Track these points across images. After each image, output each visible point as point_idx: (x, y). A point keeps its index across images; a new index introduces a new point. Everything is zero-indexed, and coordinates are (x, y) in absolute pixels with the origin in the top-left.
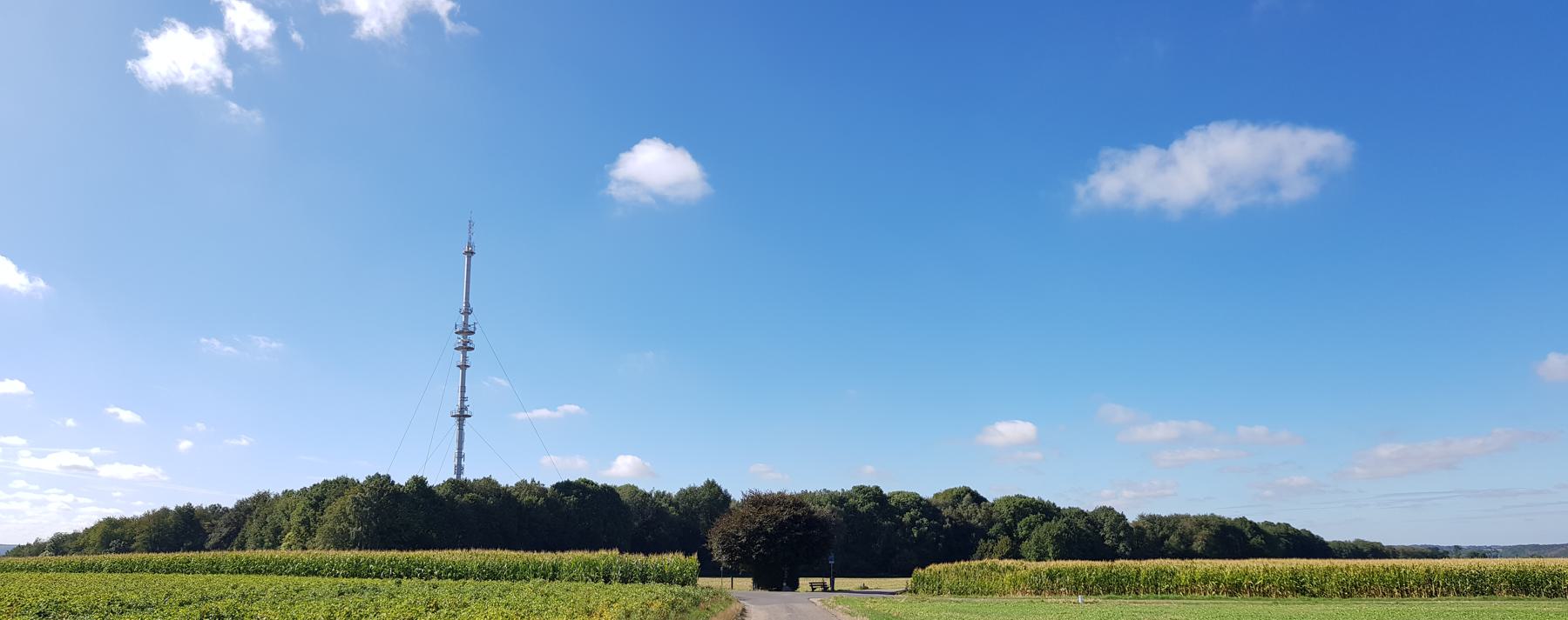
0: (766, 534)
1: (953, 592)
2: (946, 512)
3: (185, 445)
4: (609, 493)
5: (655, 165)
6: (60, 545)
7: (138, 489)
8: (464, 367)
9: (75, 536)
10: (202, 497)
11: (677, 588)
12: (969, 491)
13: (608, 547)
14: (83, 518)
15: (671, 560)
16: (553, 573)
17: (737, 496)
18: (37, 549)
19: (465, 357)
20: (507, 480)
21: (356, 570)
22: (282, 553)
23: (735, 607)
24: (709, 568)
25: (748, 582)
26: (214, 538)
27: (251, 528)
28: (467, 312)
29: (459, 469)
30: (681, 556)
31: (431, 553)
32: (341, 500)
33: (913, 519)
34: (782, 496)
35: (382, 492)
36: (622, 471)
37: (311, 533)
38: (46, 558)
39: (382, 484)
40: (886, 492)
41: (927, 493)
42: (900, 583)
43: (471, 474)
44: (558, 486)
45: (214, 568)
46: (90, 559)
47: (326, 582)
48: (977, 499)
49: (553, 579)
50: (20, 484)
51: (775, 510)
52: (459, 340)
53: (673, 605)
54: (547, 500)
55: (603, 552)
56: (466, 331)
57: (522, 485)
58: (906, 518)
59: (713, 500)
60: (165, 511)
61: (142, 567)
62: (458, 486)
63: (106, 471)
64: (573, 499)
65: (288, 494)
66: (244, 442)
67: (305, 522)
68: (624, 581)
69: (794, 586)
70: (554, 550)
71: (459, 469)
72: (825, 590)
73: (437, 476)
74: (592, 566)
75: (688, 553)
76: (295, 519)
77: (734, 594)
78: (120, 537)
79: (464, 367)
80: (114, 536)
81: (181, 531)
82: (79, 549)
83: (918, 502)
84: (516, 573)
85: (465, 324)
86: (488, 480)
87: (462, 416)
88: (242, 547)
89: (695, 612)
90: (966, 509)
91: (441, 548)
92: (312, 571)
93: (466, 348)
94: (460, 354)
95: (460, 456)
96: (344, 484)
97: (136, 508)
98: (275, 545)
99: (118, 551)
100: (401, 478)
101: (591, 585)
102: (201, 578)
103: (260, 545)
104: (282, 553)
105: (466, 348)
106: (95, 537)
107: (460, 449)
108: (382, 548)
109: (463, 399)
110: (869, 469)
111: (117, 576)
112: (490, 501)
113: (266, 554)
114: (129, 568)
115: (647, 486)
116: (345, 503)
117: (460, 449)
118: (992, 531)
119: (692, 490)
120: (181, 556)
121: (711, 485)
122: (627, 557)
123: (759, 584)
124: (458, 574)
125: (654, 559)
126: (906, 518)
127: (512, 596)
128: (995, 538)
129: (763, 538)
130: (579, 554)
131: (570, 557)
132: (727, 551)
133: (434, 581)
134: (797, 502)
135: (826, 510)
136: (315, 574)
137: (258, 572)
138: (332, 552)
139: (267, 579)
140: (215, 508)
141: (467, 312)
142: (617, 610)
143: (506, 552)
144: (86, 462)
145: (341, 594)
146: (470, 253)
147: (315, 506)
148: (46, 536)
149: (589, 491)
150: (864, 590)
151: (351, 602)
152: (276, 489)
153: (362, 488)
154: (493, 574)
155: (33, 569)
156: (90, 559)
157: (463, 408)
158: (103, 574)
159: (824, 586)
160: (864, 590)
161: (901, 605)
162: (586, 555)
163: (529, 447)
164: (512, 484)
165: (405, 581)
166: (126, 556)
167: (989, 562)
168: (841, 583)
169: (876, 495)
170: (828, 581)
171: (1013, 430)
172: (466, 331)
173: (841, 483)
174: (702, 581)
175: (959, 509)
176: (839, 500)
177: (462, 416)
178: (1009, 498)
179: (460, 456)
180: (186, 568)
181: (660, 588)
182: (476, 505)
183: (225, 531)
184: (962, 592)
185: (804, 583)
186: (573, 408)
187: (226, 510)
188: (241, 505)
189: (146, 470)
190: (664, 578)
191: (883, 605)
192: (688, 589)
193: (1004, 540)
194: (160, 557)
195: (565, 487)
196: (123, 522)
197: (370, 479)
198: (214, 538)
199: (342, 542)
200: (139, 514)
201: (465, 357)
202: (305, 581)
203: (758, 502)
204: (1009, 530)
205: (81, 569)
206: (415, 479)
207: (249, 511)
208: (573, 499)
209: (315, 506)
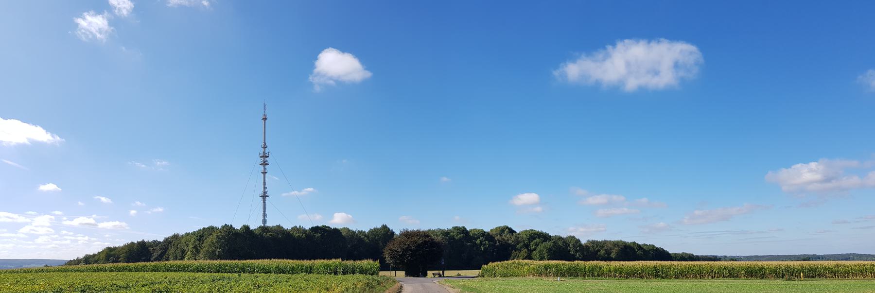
0: (411, 250)
1: (501, 276)
2: (497, 238)
3: (133, 212)
4: (336, 231)
5: (335, 63)
6: (88, 260)
7: (119, 233)
8: (264, 173)
9: (94, 255)
10: (149, 238)
11: (371, 277)
12: (507, 227)
13: (336, 258)
14: (96, 247)
15: (366, 263)
16: (310, 270)
17: (397, 232)
18: (78, 262)
20: (287, 226)
21: (219, 269)
22: (186, 262)
23: (397, 285)
24: (384, 267)
25: (404, 273)
26: (155, 256)
27: (171, 251)
28: (265, 147)
29: (264, 221)
30: (371, 261)
31: (253, 261)
32: (211, 237)
33: (481, 242)
34: (418, 232)
35: (229, 233)
36: (338, 221)
37: (198, 252)
38: (82, 266)
39: (228, 230)
40: (468, 229)
41: (487, 229)
42: (476, 272)
43: (270, 223)
45: (156, 269)
46: (101, 266)
47: (206, 275)
48: (512, 231)
49: (310, 273)
50: (64, 232)
51: (415, 238)
52: (261, 160)
53: (367, 284)
54: (307, 235)
55: (334, 260)
56: (265, 156)
57: (295, 229)
58: (478, 241)
59: (385, 234)
60: (133, 243)
61: (124, 269)
62: (264, 229)
63: (101, 225)
64: (319, 235)
65: (187, 234)
66: (160, 210)
67: (195, 247)
68: (344, 273)
69: (425, 275)
70: (310, 259)
71: (264, 221)
72: (440, 276)
73: (255, 224)
74: (327, 267)
75: (375, 260)
76: (191, 246)
77: (396, 278)
78: (114, 255)
80: (110, 255)
81: (140, 253)
82: (96, 262)
83: (483, 234)
84: (293, 271)
85: (264, 152)
86: (279, 226)
87: (264, 196)
88: (167, 259)
89: (378, 288)
90: (506, 236)
91: (258, 259)
92: (199, 270)
93: (265, 164)
94: (262, 167)
95: (265, 215)
96: (212, 229)
97: (119, 242)
98: (182, 258)
99: (113, 262)
100: (238, 226)
101: (328, 276)
102: (151, 274)
103: (176, 258)
104: (186, 262)
105: (265, 164)
106: (103, 256)
107: (264, 212)
108: (231, 259)
109: (265, 188)
111: (114, 273)
112: (280, 236)
113: (178, 262)
114: (119, 270)
115: (354, 228)
116: (213, 238)
117: (264, 212)
118: (518, 247)
119: (376, 230)
120: (141, 264)
121: (385, 227)
122: (345, 262)
123: (408, 274)
124: (267, 271)
125: (358, 263)
126: (478, 241)
127: (292, 282)
128: (520, 250)
129: (409, 252)
130: (322, 261)
131: (318, 262)
132: (392, 258)
133: (256, 274)
134: (426, 235)
135: (440, 238)
136: (201, 271)
137: (175, 271)
138: (208, 261)
139: (180, 274)
140: (154, 242)
141: (265, 147)
142: (341, 288)
143: (288, 261)
144: (92, 221)
145: (214, 281)
146: (265, 119)
147: (200, 240)
148: (81, 256)
149: (327, 231)
150: (459, 276)
151: (219, 284)
152: (182, 232)
153: (220, 231)
154: (281, 271)
155: (76, 271)
156: (101, 266)
157: (265, 193)
158: (108, 273)
159: (439, 274)
160: (459, 276)
161: (477, 283)
162: (325, 261)
163: (296, 210)
164: (290, 228)
165: (242, 274)
166: (116, 264)
167: (517, 261)
168: (447, 273)
169: (464, 231)
170: (441, 272)
171: (528, 198)
172: (265, 156)
173: (447, 226)
174: (381, 273)
175: (503, 236)
176: (446, 233)
177: (264, 196)
178: (526, 231)
179: (265, 215)
180: (143, 269)
181: (361, 276)
182: (274, 239)
183: (160, 252)
184: (505, 276)
185: (430, 273)
187: (160, 242)
188: (166, 239)
189: (117, 223)
190: (363, 271)
191: (468, 283)
192: (375, 277)
193: (524, 251)
194: (131, 264)
195: (315, 229)
196: (115, 249)
197: (223, 227)
198: (155, 256)
199: (213, 256)
200: (122, 245)
202: (197, 275)
203: (407, 235)
204: (527, 246)
205: (97, 270)
206: (244, 226)
207: (170, 243)
208: (319, 235)
209: (200, 240)
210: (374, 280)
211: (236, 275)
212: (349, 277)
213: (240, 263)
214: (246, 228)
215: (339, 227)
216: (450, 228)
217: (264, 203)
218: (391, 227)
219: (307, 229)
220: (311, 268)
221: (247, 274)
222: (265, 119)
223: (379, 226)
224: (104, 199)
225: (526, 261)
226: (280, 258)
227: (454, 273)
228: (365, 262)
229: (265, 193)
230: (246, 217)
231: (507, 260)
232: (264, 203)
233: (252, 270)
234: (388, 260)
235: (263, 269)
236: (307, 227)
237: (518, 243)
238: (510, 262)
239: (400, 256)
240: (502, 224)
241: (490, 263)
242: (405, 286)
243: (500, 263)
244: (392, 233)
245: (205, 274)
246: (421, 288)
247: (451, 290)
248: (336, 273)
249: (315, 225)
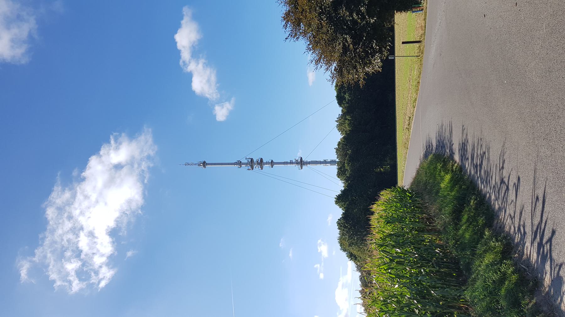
8: (272, 163)
19: (267, 163)
20: (338, 136)
28: (239, 163)
29: (332, 162)
43: (334, 156)
44: (340, 103)
52: (257, 168)
56: (251, 163)
57: (340, 126)
64: (347, 96)
71: (332, 162)
79: (272, 163)
85: (246, 164)
87: (301, 163)
93: (261, 163)
94: (266, 167)
107: (320, 163)
109: (291, 163)
117: (320, 163)
141: (239, 163)
146: (204, 164)
157: (297, 163)
172: (251, 163)
177: (301, 163)
179: (325, 162)
182: (352, 159)
201: (267, 163)
208: (347, 96)
214: (340, 199)
217: (309, 163)
222: (204, 164)
232: (309, 163)
236: (338, 110)
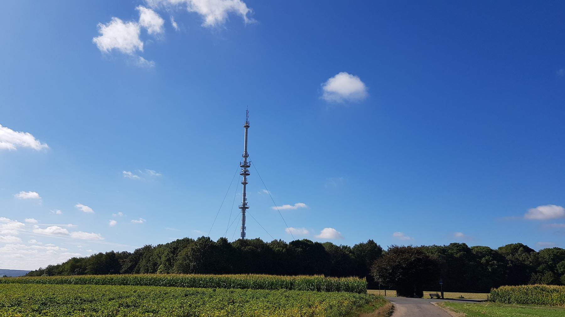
0: (402, 268)
1: (518, 302)
2: (509, 257)
3: (113, 223)
4: (318, 246)
6: (51, 271)
7: (89, 244)
8: (245, 183)
9: (58, 266)
10: (118, 248)
11: (357, 295)
12: (521, 245)
13: (319, 273)
14: (61, 258)
15: (351, 280)
16: (291, 286)
17: (385, 248)
18: (40, 273)
19: (245, 179)
20: (267, 239)
21: (193, 284)
22: (158, 275)
23: (388, 305)
24: (372, 285)
25: (394, 293)
26: (125, 268)
27: (142, 263)
28: (246, 156)
29: (243, 234)
30: (357, 279)
31: (229, 276)
32: (185, 249)
33: (487, 261)
34: (410, 248)
35: (205, 246)
36: (326, 235)
37: (171, 265)
38: (44, 277)
39: (205, 242)
40: (469, 246)
41: (494, 247)
42: (483, 296)
43: (249, 236)
44: (293, 243)
45: (124, 283)
46: (65, 277)
47: (179, 289)
48: (527, 250)
49: (290, 289)
50: (34, 241)
51: (406, 256)
52: (242, 170)
53: (354, 303)
54: (287, 250)
55: (316, 276)
56: (246, 166)
57: (275, 242)
58: (483, 260)
59: (371, 250)
60: (101, 254)
61: (90, 282)
62: (243, 242)
63: (75, 235)
64: (299, 249)
65: (160, 246)
66: (141, 221)
67: (168, 260)
68: (328, 290)
69: (421, 296)
70: (291, 275)
71: (243, 234)
72: (438, 298)
73: (233, 237)
74: (309, 283)
75: (361, 277)
76: (164, 259)
77: (387, 298)
78: (80, 267)
79: (245, 183)
80: (76, 266)
81: (108, 265)
82: (60, 273)
83: (489, 252)
84: (272, 286)
85: (245, 162)
86: (258, 240)
87: (244, 208)
88: (138, 272)
89: (367, 307)
90: (521, 256)
91: (235, 273)
92: (171, 284)
93: (246, 174)
95: (244, 228)
96: (187, 242)
97: (86, 253)
98: (154, 271)
99: (79, 274)
100: (215, 239)
101: (310, 293)
102: (119, 287)
103: (147, 271)
104: (158, 275)
105: (246, 174)
106: (67, 267)
107: (244, 224)
108: (206, 273)
109: (245, 199)
110: (460, 234)
111: (79, 286)
112: (259, 250)
113: (150, 276)
114: (84, 282)
115: (338, 243)
116: (188, 250)
117: (244, 224)
118: (540, 268)
119: (361, 245)
120: (109, 276)
121: (371, 242)
122: (329, 279)
123: (400, 294)
124: (244, 286)
125: (343, 280)
126: (483, 260)
127: (271, 298)
128: (542, 273)
129: (401, 270)
130: (304, 277)
131: (299, 278)
132: (381, 276)
133: (232, 289)
134: (419, 251)
135: (435, 256)
136: (173, 285)
137: (146, 284)
138: (182, 275)
139: (151, 288)
140: (124, 253)
141: (246, 156)
142: (324, 305)
143: (267, 276)
144: (64, 231)
145: (186, 295)
146: (247, 127)
147: (173, 252)
148: (44, 267)
149: (308, 245)
150: (462, 299)
152: (154, 244)
153: (195, 243)
154: (259, 286)
155: (38, 282)
156: (65, 277)
157: (245, 204)
158: (72, 286)
159: (437, 295)
160: (462, 299)
161: (486, 308)
162: (307, 277)
163: (279, 224)
164: (269, 242)
165: (217, 289)
166: (83, 276)
167: (541, 286)
168: (447, 295)
169: (463, 248)
170: (440, 293)
171: (548, 211)
172: (246, 166)
173: (444, 242)
174: (369, 291)
175: (517, 255)
176: (442, 251)
177: (244, 208)
178: (549, 250)
179: (244, 228)
180: (111, 282)
181: (347, 294)
183: (130, 264)
184: (525, 303)
185: (426, 294)
186: (302, 205)
187: (130, 254)
188: (137, 251)
189: (93, 235)
190: (349, 289)
191: (475, 308)
192: (362, 295)
193: (549, 275)
194: (99, 277)
195: (296, 243)
196: (81, 260)
197: (199, 239)
198: (125, 268)
199: (186, 270)
200: (89, 256)
201: (245, 179)
202: (169, 289)
203: (396, 251)
204: (552, 268)
205: (62, 282)
206: (222, 239)
207: (141, 254)
208: (299, 249)
209: (173, 252)
210: (361, 298)
211: (210, 290)
212: (335, 294)
213: (216, 277)
215: (322, 242)
216: (447, 244)
217: (244, 215)
218: (378, 242)
219: (352, 247)
220: (292, 284)
221: (222, 289)
222: (247, 127)
223: (365, 242)
224: (85, 208)
225: (552, 287)
226: (257, 273)
227: (457, 295)
228: (351, 279)
229: (245, 204)
230: (225, 229)
231: (526, 284)
232: (244, 215)
233: (228, 285)
234: (377, 277)
235: (240, 284)
236: (288, 241)
237: (539, 264)
238: (530, 286)
239: (389, 274)
240: (515, 241)
241: (501, 287)
242: (397, 306)
243: (517, 287)
244: (380, 249)
245: (177, 289)
246: (416, 310)
247: (453, 314)
248: (319, 290)
249: (295, 239)
